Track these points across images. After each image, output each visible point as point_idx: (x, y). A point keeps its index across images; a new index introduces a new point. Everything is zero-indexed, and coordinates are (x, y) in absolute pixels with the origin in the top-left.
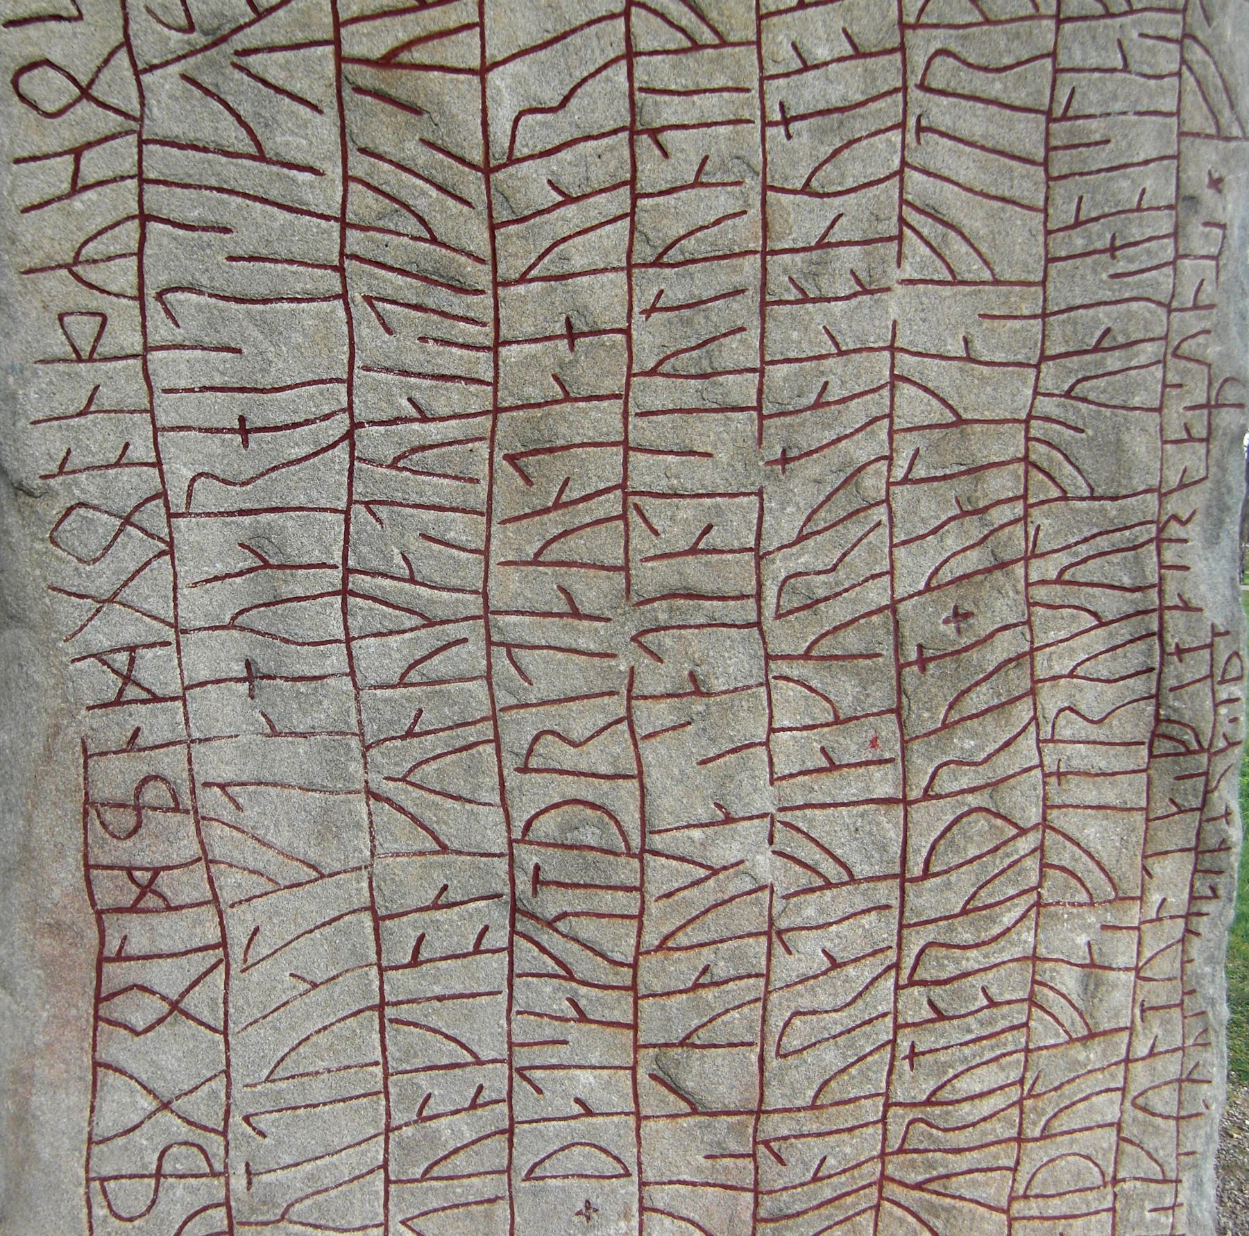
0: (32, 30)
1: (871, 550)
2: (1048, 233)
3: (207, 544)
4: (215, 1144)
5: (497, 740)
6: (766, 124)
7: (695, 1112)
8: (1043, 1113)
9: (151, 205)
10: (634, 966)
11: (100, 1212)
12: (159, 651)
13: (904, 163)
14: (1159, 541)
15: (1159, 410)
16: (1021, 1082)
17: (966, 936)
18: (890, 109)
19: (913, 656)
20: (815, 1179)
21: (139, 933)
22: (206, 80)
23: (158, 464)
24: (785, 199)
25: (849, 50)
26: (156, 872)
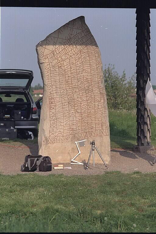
3: (54, 87)
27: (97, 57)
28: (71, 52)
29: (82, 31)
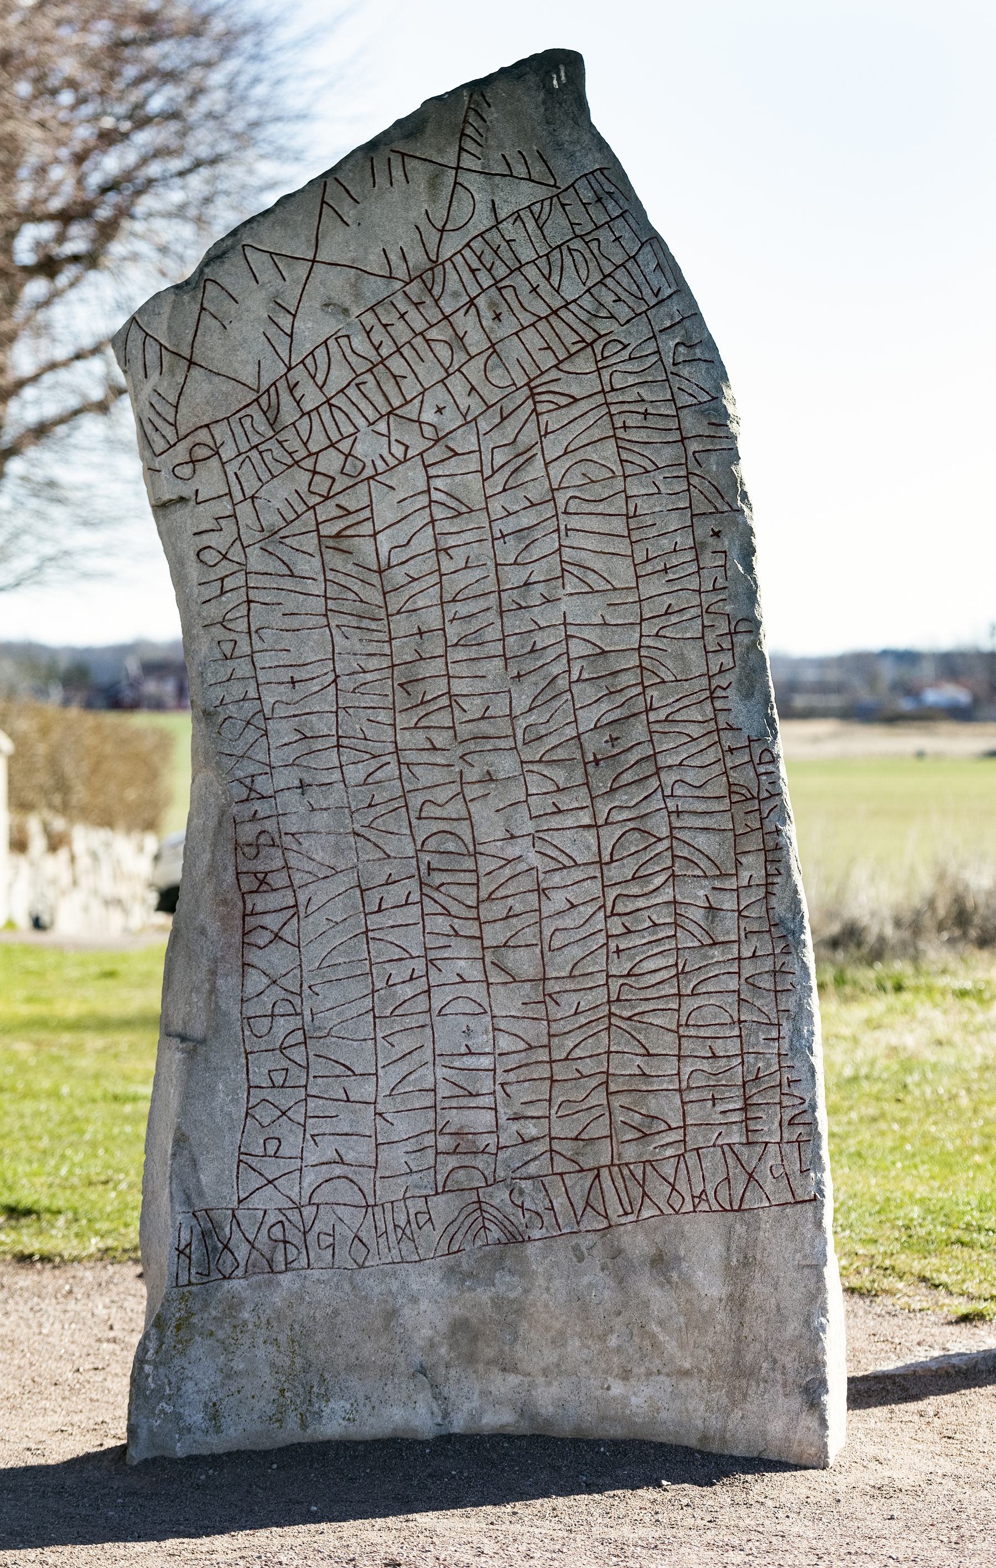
0: (204, 536)
1: (564, 711)
2: (635, 565)
4: (297, 1001)
5: (406, 805)
6: (493, 539)
7: (515, 981)
8: (690, 981)
9: (251, 598)
10: (477, 907)
11: (247, 1033)
12: (264, 776)
13: (560, 545)
14: (712, 698)
15: (703, 638)
16: (676, 965)
17: (635, 890)
18: (552, 525)
19: (592, 758)
20: (576, 1013)
21: (261, 902)
22: (270, 549)
23: (260, 698)
24: (506, 568)
25: (528, 504)
26: (266, 874)
27: (694, 446)
28: (438, 396)
29: (542, 192)
